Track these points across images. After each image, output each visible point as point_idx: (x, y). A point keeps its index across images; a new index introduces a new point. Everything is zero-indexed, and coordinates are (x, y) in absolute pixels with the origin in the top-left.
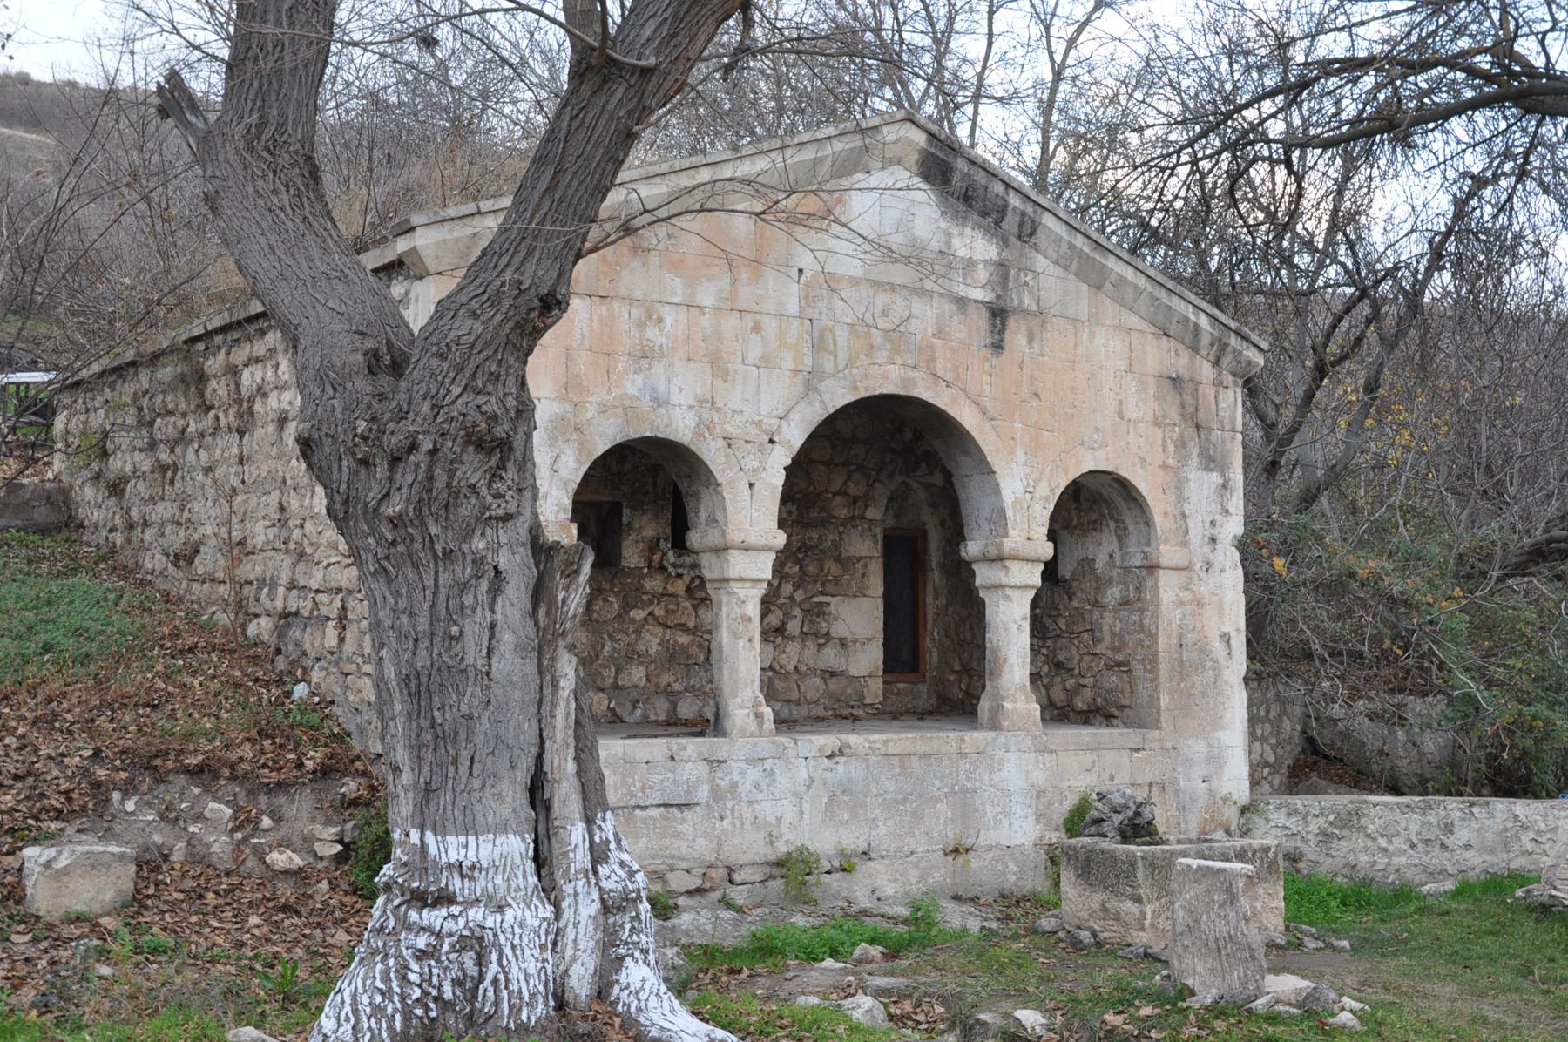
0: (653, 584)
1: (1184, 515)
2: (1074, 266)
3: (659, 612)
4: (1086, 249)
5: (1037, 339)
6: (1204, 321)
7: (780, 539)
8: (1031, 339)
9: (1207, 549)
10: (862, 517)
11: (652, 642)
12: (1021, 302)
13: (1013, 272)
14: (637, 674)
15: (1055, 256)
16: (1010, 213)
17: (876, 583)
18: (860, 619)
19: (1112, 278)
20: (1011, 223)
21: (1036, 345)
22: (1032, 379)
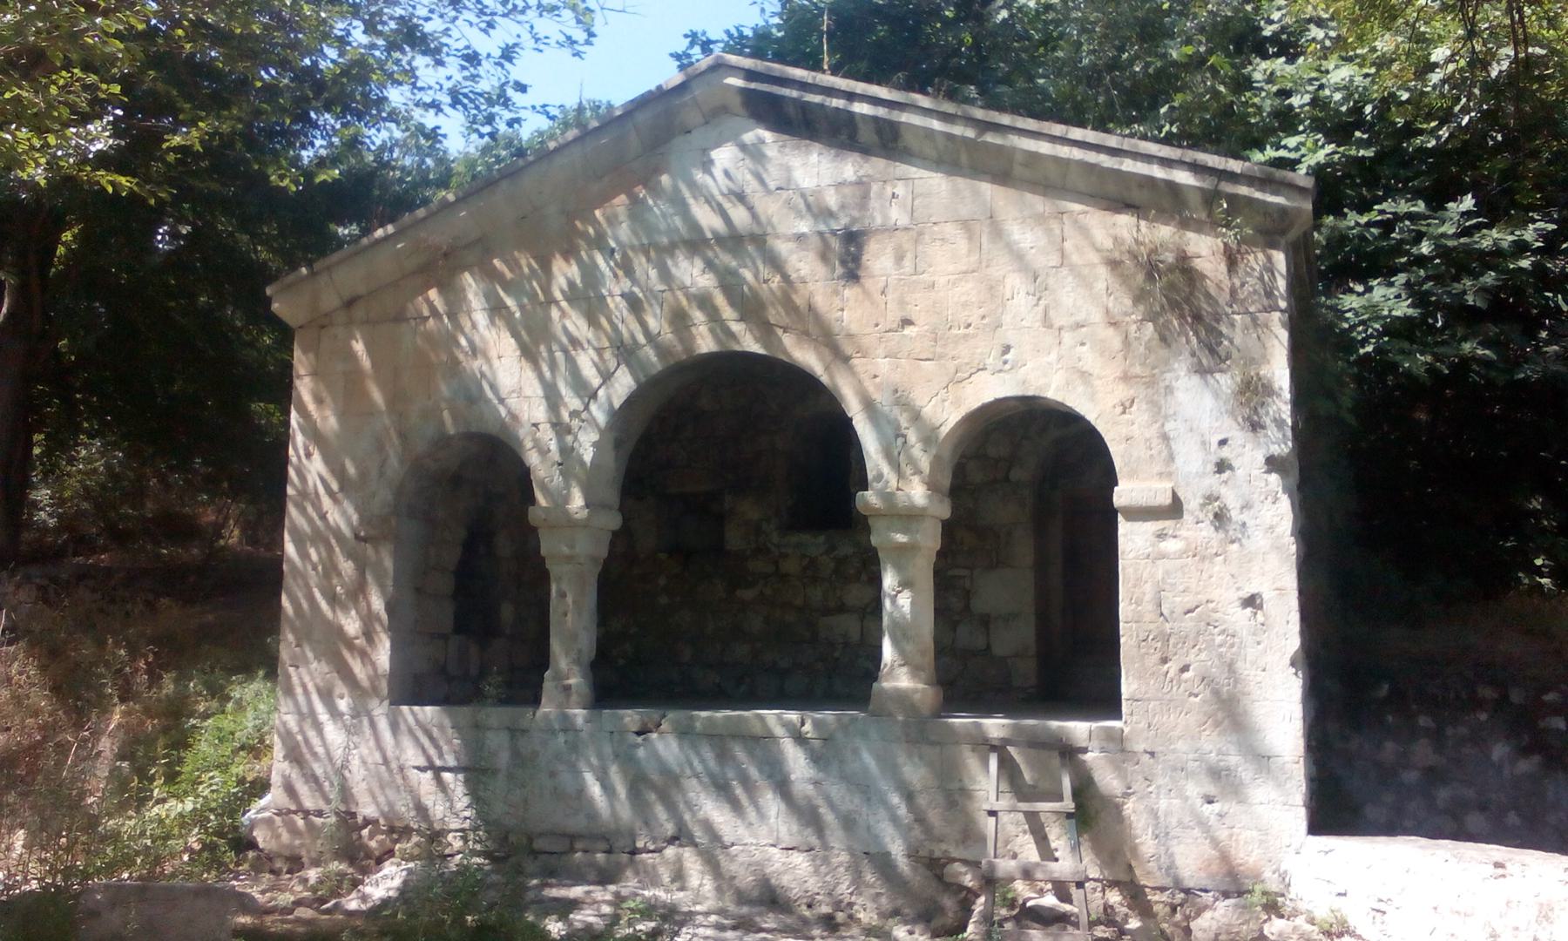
0: (758, 565)
1: (1165, 438)
2: (964, 158)
3: (768, 591)
4: (970, 133)
5: (909, 256)
6: (1183, 177)
7: (945, 511)
8: (899, 258)
9: (1212, 482)
10: (1007, 479)
11: (755, 623)
12: (886, 217)
13: (875, 187)
14: (741, 651)
15: (934, 154)
16: (861, 125)
17: (1024, 550)
18: (1008, 593)
19: (1019, 157)
20: (866, 135)
21: (908, 263)
22: (902, 303)
